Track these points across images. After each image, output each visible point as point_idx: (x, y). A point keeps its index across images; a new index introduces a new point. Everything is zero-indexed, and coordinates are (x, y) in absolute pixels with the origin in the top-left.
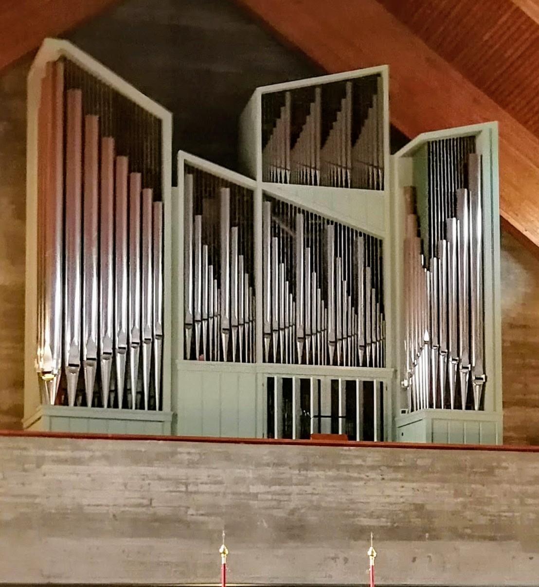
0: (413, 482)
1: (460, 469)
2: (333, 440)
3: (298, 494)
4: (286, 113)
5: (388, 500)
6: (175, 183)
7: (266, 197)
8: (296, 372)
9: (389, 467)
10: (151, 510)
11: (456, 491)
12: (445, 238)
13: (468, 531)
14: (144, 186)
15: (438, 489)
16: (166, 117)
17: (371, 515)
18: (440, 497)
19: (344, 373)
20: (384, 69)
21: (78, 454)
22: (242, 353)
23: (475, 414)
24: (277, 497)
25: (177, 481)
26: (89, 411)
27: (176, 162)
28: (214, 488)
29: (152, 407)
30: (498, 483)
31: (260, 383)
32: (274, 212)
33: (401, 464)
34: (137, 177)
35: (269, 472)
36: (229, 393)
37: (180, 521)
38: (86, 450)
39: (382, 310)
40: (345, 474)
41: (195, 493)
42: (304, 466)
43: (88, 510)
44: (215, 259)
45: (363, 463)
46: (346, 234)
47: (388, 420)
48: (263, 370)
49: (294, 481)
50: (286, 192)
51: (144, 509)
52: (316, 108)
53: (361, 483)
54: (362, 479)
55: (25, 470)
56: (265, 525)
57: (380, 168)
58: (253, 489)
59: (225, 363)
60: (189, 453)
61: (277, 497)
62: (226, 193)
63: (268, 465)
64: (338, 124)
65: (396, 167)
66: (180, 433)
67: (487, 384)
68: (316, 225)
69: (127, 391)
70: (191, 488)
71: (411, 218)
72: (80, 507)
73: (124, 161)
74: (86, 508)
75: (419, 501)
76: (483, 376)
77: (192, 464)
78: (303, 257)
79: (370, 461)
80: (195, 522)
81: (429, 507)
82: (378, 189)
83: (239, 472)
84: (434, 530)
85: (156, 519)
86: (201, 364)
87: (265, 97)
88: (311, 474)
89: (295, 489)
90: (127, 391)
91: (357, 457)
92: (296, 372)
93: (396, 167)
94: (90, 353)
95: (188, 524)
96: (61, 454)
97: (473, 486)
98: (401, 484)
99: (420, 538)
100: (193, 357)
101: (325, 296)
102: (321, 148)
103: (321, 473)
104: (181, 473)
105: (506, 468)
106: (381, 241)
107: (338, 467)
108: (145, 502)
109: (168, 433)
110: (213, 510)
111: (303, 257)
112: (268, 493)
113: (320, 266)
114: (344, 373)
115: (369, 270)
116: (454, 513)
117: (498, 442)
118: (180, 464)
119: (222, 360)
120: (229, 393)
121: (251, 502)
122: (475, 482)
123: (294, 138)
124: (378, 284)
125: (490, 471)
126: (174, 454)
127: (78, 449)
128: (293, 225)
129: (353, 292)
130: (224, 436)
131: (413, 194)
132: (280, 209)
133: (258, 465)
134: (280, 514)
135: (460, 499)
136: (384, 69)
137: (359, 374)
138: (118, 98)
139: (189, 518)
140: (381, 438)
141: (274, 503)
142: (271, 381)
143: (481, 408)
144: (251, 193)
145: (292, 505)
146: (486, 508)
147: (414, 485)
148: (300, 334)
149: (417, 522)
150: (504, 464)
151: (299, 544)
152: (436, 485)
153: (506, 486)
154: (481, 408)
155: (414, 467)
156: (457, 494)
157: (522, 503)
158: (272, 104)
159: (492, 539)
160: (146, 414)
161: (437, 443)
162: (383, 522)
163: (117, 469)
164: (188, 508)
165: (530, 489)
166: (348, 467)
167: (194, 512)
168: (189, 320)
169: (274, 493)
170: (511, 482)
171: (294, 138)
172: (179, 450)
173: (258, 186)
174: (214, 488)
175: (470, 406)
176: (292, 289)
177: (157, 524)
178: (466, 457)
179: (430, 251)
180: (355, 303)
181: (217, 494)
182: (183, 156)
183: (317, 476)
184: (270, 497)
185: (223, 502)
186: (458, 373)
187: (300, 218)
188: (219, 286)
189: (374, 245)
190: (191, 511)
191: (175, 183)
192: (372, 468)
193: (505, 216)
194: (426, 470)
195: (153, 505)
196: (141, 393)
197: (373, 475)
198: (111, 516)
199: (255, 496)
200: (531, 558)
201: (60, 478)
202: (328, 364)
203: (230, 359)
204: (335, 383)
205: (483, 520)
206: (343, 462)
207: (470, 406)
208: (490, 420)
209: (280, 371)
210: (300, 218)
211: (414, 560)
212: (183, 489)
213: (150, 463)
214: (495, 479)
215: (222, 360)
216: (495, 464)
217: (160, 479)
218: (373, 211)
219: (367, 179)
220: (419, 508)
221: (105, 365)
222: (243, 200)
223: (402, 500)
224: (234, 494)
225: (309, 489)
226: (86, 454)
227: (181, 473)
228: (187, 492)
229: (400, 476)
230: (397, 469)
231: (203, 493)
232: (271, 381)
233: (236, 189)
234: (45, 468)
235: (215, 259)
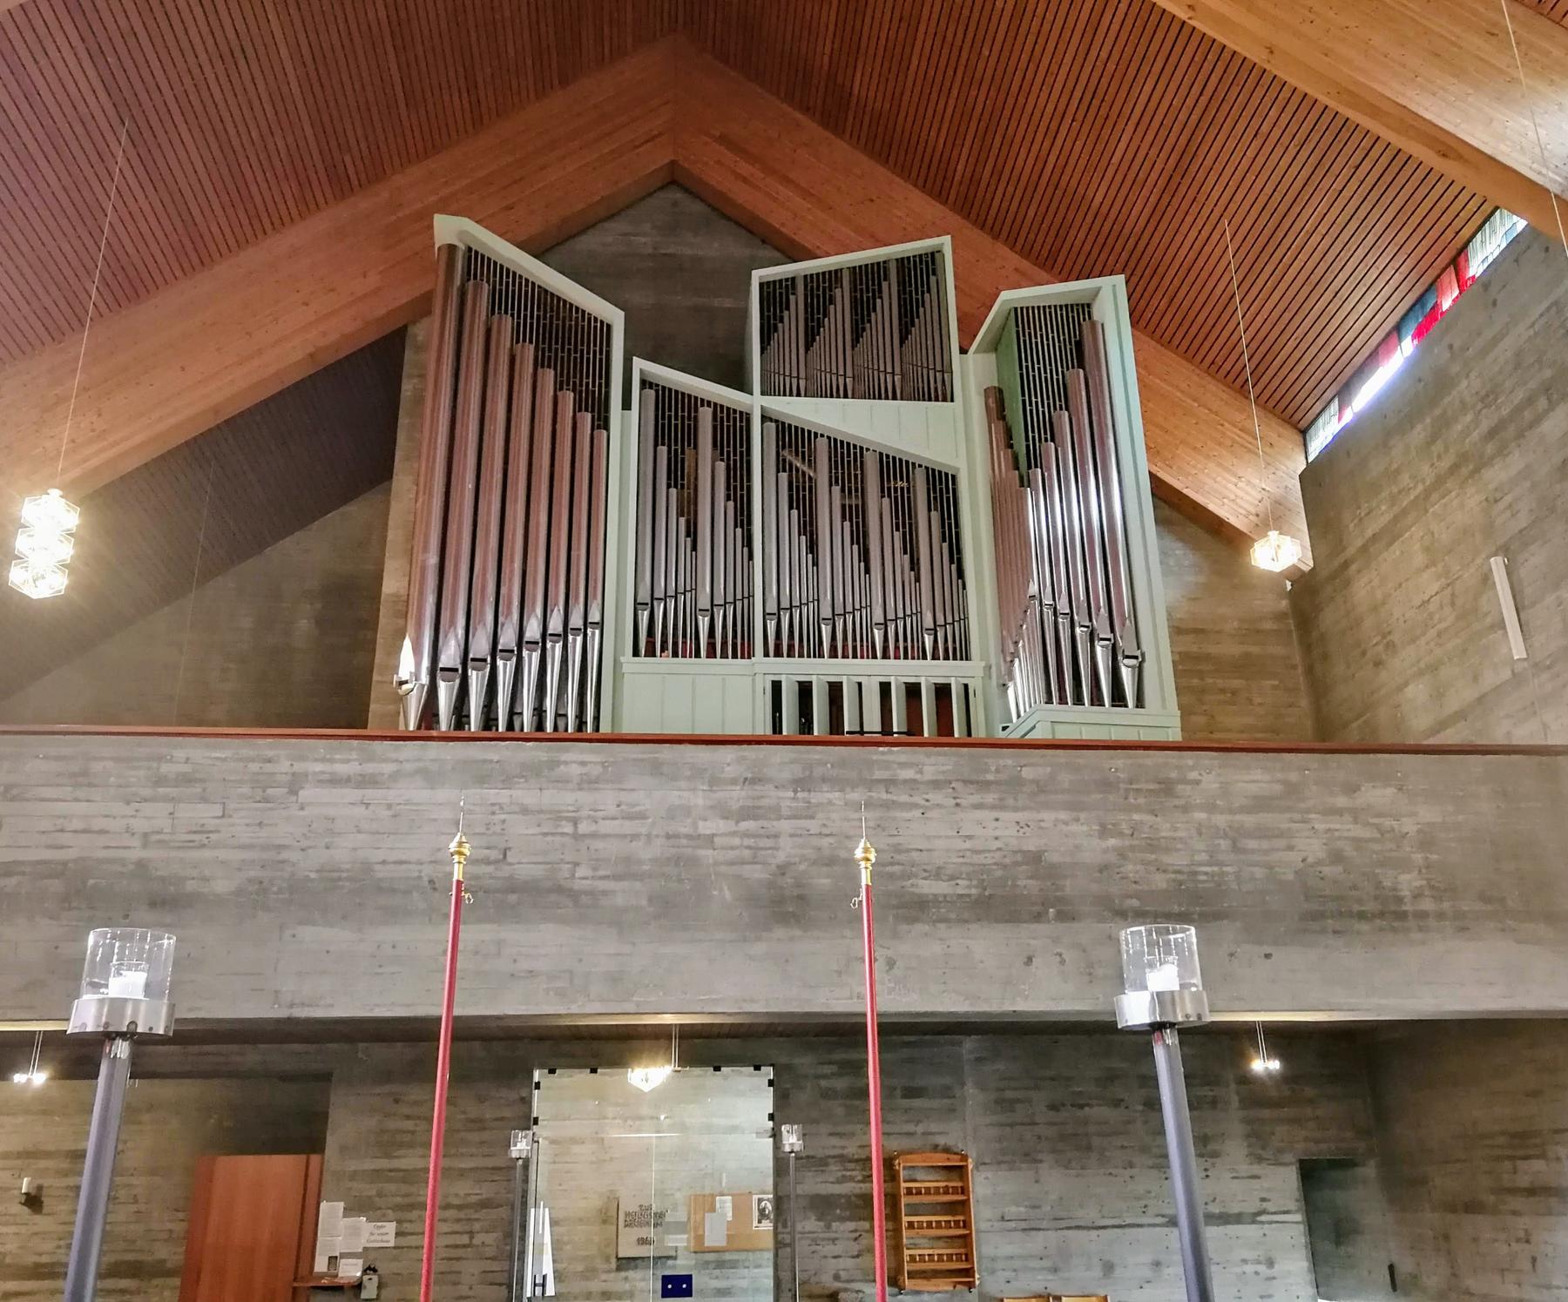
0: (1016, 809)
1: (1106, 785)
3: (791, 836)
5: (968, 845)
6: (626, 405)
8: (820, 671)
9: (965, 782)
10: (505, 871)
11: (1103, 826)
12: (1053, 440)
13: (1135, 903)
14: (579, 407)
15: (1066, 823)
16: (616, 318)
17: (937, 874)
19: (900, 671)
20: (946, 242)
21: (370, 768)
24: (751, 842)
25: (557, 816)
27: (630, 371)
28: (629, 827)
30: (1186, 809)
31: (759, 690)
32: (781, 444)
33: (990, 777)
34: (568, 398)
35: (737, 796)
37: (559, 890)
38: (386, 760)
39: (961, 574)
40: (885, 796)
41: (594, 836)
42: (800, 784)
43: (381, 872)
45: (918, 777)
46: (894, 468)
48: (765, 668)
49: (785, 812)
51: (490, 869)
53: (917, 813)
54: (916, 806)
55: (266, 800)
56: (728, 895)
57: (947, 369)
58: (705, 828)
59: (703, 659)
60: (583, 764)
61: (751, 842)
62: (706, 414)
63: (734, 782)
65: (973, 372)
67: (1146, 665)
68: (846, 455)
70: (584, 828)
71: (998, 427)
72: (367, 867)
73: (548, 376)
74: (377, 867)
75: (1031, 845)
76: (1138, 653)
77: (588, 783)
79: (930, 773)
80: (591, 893)
81: (1053, 857)
82: (945, 400)
83: (675, 797)
84: (1061, 900)
85: (513, 886)
86: (664, 662)
88: (816, 798)
89: (785, 826)
91: (903, 765)
92: (820, 671)
93: (973, 372)
95: (574, 895)
96: (341, 769)
97: (1136, 817)
98: (995, 814)
99: (1038, 917)
100: (651, 652)
102: (853, 348)
103: (835, 796)
104: (567, 799)
105: (1198, 782)
106: (954, 477)
107: (871, 784)
108: (495, 855)
110: (626, 870)
112: (734, 834)
113: (855, 515)
114: (900, 671)
115: (935, 515)
116: (1103, 868)
118: (563, 781)
119: (698, 655)
121: (707, 854)
122: (1138, 809)
125: (1166, 788)
126: (553, 764)
127: (371, 759)
129: (910, 547)
131: (997, 402)
132: (791, 438)
133: (714, 782)
134: (757, 873)
135: (1112, 842)
136: (946, 242)
137: (928, 672)
138: (548, 300)
139: (578, 885)
141: (747, 853)
142: (777, 687)
143: (1140, 703)
144: (746, 417)
145: (781, 857)
146: (1167, 859)
147: (1019, 816)
148: (826, 612)
149: (1029, 885)
150: (1193, 775)
151: (798, 932)
152: (1063, 815)
153: (1200, 816)
154: (1140, 703)
155: (1014, 783)
156: (1104, 832)
157: (1235, 848)
158: (775, 295)
162: (963, 887)
163: (443, 794)
164: (576, 864)
165: (1249, 820)
166: (890, 783)
167: (589, 873)
168: (644, 596)
169: (746, 834)
170: (1211, 808)
172: (565, 757)
173: (754, 402)
174: (629, 827)
177: (513, 898)
178: (1120, 760)
180: (914, 565)
181: (635, 837)
182: (639, 364)
183: (830, 802)
184: (736, 841)
185: (646, 852)
187: (822, 445)
188: (694, 548)
190: (581, 872)
191: (626, 405)
192: (936, 784)
193: (1155, 470)
194: (1041, 788)
195: (509, 859)
197: (936, 797)
198: (426, 879)
199: (709, 840)
200: (1268, 956)
201: (331, 812)
202: (875, 657)
203: (711, 653)
204: (885, 688)
205: (1160, 882)
206: (879, 774)
209: (792, 670)
211: (1029, 960)
212: (568, 829)
213: (508, 781)
214: (1177, 802)
215: (698, 655)
216: (1174, 775)
217: (525, 811)
220: (1035, 858)
222: (732, 428)
223: (998, 844)
224: (668, 837)
225: (813, 826)
226: (388, 768)
227: (567, 799)
228: (576, 836)
229: (990, 798)
230: (985, 785)
231: (606, 836)
232: (777, 687)
233: (717, 408)
234: (304, 794)
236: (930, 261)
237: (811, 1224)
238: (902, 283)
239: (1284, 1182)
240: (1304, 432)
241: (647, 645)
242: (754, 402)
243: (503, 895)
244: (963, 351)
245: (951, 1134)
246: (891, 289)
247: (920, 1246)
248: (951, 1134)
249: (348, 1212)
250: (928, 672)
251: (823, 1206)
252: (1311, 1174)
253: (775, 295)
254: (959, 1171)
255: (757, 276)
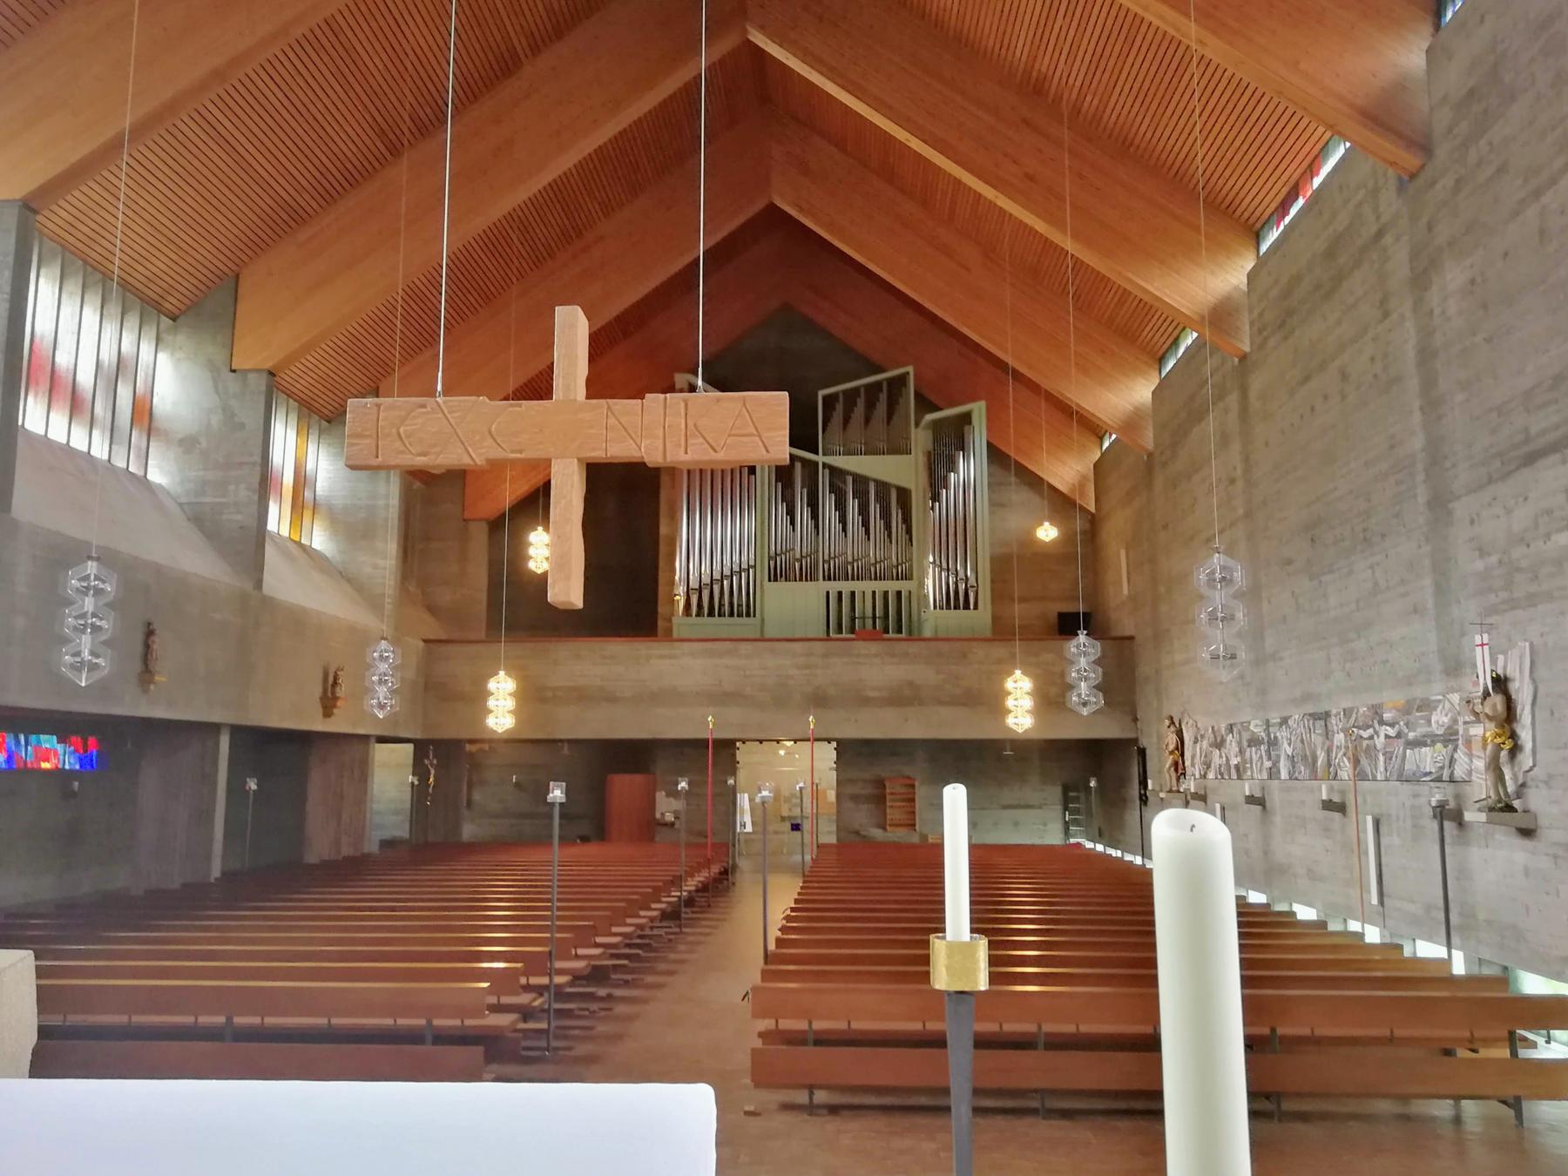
2: (873, 636)
4: (840, 407)
7: (824, 465)
8: (846, 586)
18: (925, 675)
20: (910, 369)
22: (808, 575)
23: (971, 612)
26: (706, 619)
29: (748, 615)
36: (796, 604)
42: (825, 656)
44: (791, 512)
46: (883, 488)
47: (915, 617)
48: (823, 586)
50: (830, 460)
52: (861, 403)
57: (908, 438)
64: (879, 410)
66: (768, 635)
68: (861, 482)
69: (721, 605)
78: (852, 506)
86: (782, 585)
87: (825, 398)
90: (740, 605)
93: (920, 439)
94: (706, 580)
101: (867, 532)
109: (758, 636)
111: (852, 506)
113: (864, 510)
114: (880, 586)
117: (988, 634)
120: (796, 604)
123: (867, 420)
124: (907, 520)
125: (964, 655)
128: (845, 482)
129: (888, 527)
130: (798, 635)
132: (835, 472)
136: (910, 369)
137: (892, 586)
140: (910, 632)
143: (976, 607)
144: (816, 464)
154: (976, 607)
159: (964, 705)
160: (744, 620)
161: (941, 635)
166: (858, 656)
171: (867, 420)
173: (820, 459)
175: (967, 607)
176: (844, 530)
178: (944, 646)
179: (935, 497)
186: (956, 584)
189: (904, 495)
192: (876, 655)
196: (740, 605)
207: (967, 607)
208: (980, 617)
210: (850, 479)
218: (901, 470)
219: (899, 447)
220: (911, 684)
221: (716, 588)
222: (811, 467)
230: (893, 655)
235: (791, 512)
236: (902, 379)
237: (849, 805)
238: (889, 392)
239: (1056, 792)
240: (1101, 439)
241: (774, 577)
242: (820, 459)
243: (720, 698)
244: (917, 425)
245: (907, 771)
246: (883, 397)
247: (893, 814)
248: (907, 771)
249: (668, 795)
250: (892, 586)
251: (855, 798)
252: (1066, 789)
253: (830, 401)
254: (913, 786)
255: (821, 393)
